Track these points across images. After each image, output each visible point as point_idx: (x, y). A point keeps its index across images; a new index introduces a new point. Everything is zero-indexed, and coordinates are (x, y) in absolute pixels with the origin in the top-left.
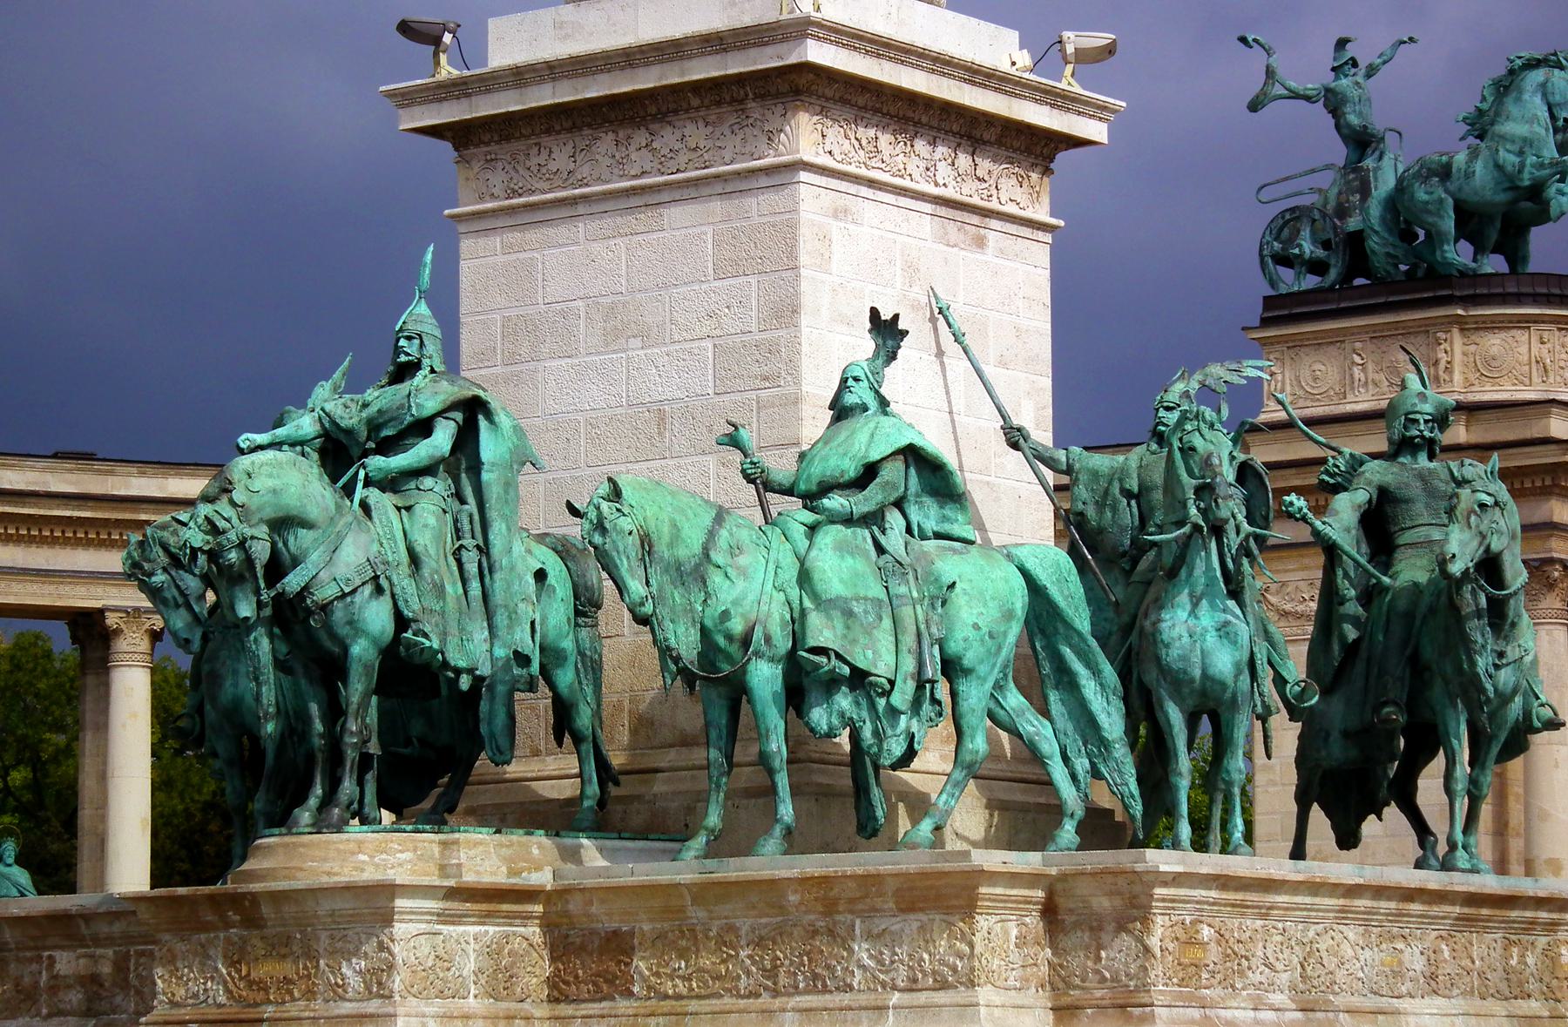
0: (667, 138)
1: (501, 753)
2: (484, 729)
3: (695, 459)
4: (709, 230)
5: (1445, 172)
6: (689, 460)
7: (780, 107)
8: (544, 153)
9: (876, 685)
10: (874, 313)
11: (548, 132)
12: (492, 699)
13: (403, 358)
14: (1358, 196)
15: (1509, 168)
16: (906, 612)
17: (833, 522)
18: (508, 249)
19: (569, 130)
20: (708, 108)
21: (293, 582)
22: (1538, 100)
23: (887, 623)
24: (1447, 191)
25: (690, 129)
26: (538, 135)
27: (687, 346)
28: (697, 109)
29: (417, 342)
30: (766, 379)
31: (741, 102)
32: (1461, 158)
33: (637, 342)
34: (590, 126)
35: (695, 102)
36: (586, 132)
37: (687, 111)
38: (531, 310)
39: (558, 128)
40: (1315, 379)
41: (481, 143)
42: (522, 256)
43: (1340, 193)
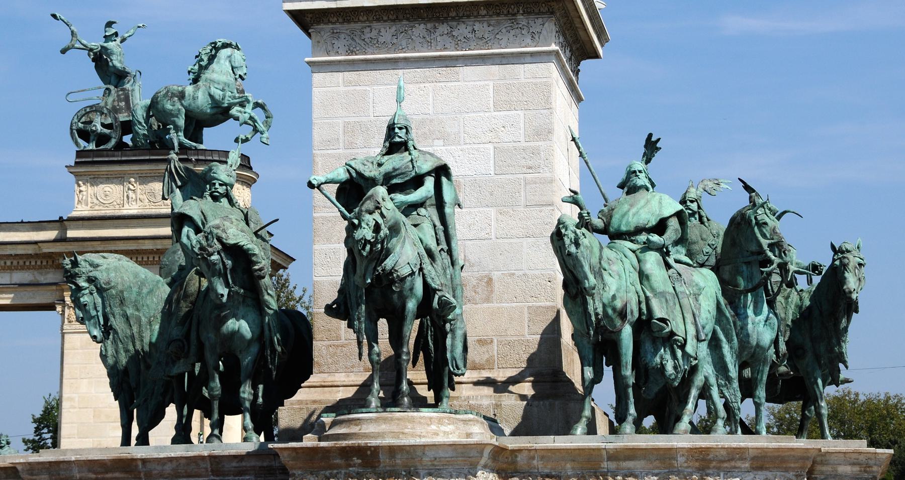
0: (463, 30)
1: (458, 369)
2: (449, 355)
3: (481, 209)
4: (491, 84)
5: (182, 96)
6: (477, 210)
7: (540, 20)
8: (374, 33)
9: (678, 340)
10: (650, 135)
11: (378, 20)
12: (453, 338)
13: (397, 139)
14: (123, 103)
15: (217, 97)
16: (685, 301)
17: (652, 250)
18: (348, 83)
19: (393, 21)
20: (491, 16)
22: (227, 63)
23: (678, 306)
24: (182, 105)
25: (477, 26)
26: (371, 22)
27: (476, 146)
28: (484, 16)
29: (404, 130)
30: (530, 168)
31: (514, 15)
32: (189, 89)
33: (441, 142)
34: (408, 19)
35: (484, 12)
36: (405, 22)
37: (476, 17)
38: (364, 119)
39: (385, 18)
40: (106, 196)
41: (329, 22)
42: (358, 88)
43: (114, 101)
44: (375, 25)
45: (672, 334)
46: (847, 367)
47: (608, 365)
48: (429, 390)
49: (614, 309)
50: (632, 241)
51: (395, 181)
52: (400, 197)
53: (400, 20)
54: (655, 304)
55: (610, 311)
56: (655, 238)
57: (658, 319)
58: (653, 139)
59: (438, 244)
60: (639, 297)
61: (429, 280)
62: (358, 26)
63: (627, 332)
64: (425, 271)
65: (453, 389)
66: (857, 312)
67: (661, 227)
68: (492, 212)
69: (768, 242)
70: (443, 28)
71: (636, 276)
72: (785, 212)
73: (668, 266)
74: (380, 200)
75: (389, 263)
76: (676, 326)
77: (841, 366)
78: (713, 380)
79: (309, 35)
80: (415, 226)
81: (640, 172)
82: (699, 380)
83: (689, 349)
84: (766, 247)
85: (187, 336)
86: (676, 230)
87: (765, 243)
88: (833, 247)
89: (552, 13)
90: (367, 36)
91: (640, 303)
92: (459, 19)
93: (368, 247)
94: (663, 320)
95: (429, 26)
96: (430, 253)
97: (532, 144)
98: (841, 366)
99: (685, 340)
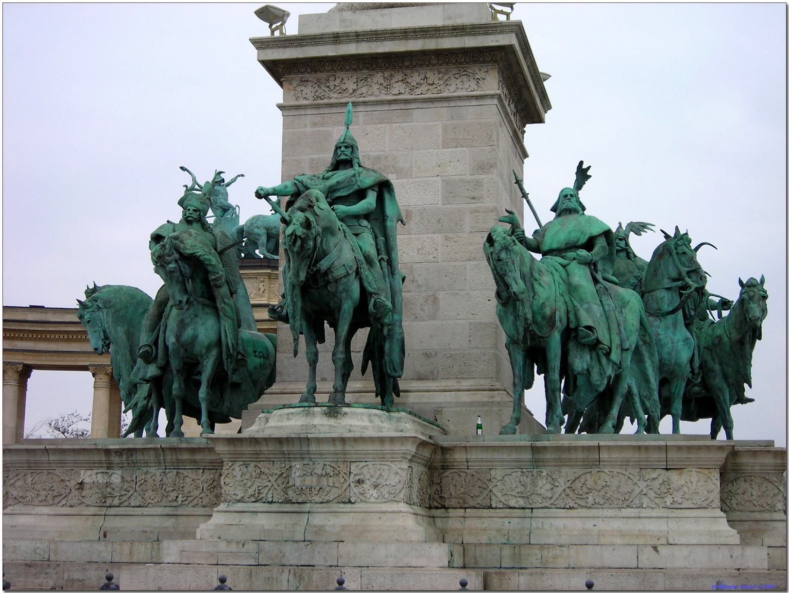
1: (395, 371)
3: (429, 235)
6: (425, 236)
9: (603, 349)
10: (581, 163)
11: (341, 70)
12: (391, 344)
18: (315, 124)
19: (355, 70)
20: (441, 65)
21: (324, 264)
26: (335, 71)
27: (425, 179)
28: (434, 65)
29: (350, 149)
30: (474, 198)
34: (368, 69)
36: (365, 71)
37: (427, 66)
41: (299, 72)
42: (322, 129)
44: (341, 74)
45: (598, 342)
46: (750, 387)
47: (539, 373)
48: (377, 396)
49: (544, 317)
50: (562, 257)
51: (338, 194)
52: (341, 208)
53: (361, 70)
54: (583, 314)
55: (539, 318)
56: (583, 253)
57: (585, 327)
58: (584, 167)
59: (378, 254)
60: (567, 307)
61: (366, 284)
62: (324, 75)
63: (556, 339)
64: (363, 276)
65: (398, 395)
66: (760, 339)
67: (589, 245)
68: (439, 238)
69: (687, 269)
71: (563, 287)
72: (702, 244)
73: (596, 281)
74: (314, 200)
75: (324, 264)
76: (602, 334)
77: (746, 385)
78: (635, 390)
79: (281, 84)
80: (356, 235)
81: (571, 196)
82: (623, 389)
83: (614, 356)
84: (684, 274)
85: (156, 343)
86: (603, 248)
88: (741, 282)
89: (495, 62)
90: (332, 83)
91: (568, 312)
92: (412, 67)
93: (299, 242)
94: (589, 328)
95: (387, 74)
96: (369, 260)
97: (477, 177)
98: (746, 385)
99: (610, 349)
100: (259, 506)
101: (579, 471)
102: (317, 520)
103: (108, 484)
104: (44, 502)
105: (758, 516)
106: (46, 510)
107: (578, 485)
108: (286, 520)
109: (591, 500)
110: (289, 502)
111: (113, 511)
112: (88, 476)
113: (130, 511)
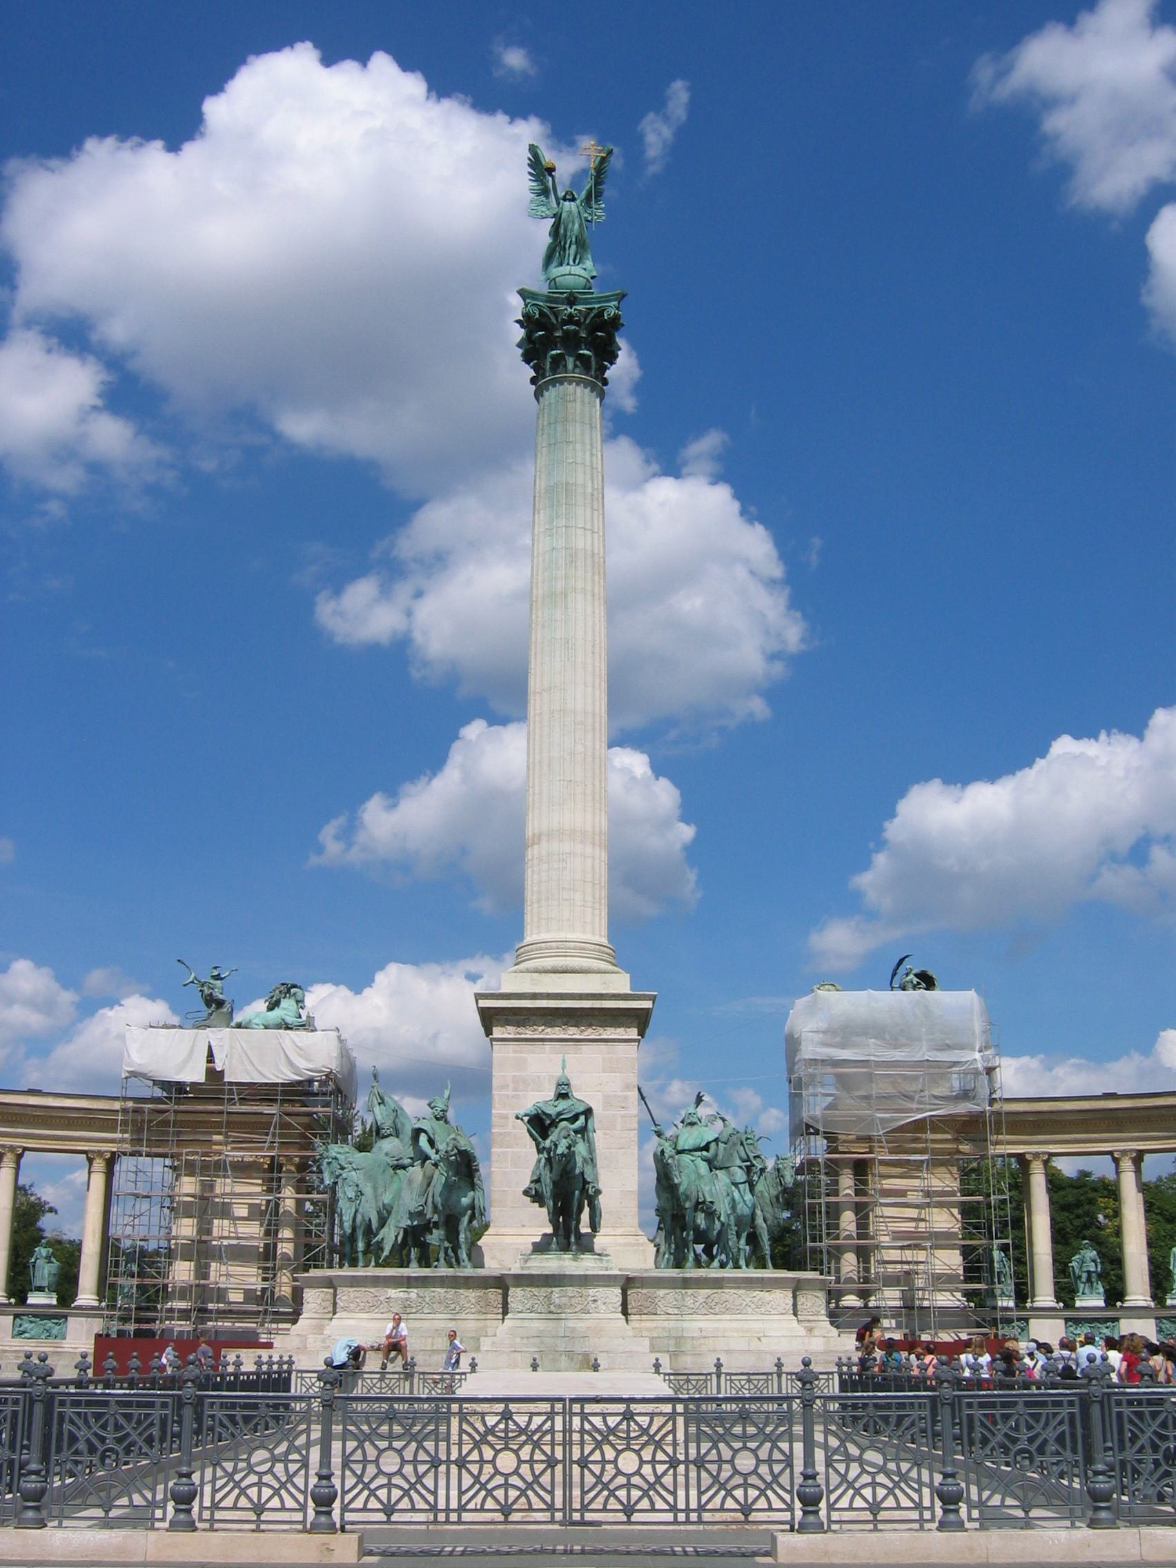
18: (515, 1052)
56: (705, 1153)
67: (706, 1148)
70: (572, 1022)
87: (751, 1155)
100: (533, 1315)
101: (709, 1291)
102: (570, 1324)
103: (407, 1299)
104: (362, 1310)
105: (811, 1318)
106: (365, 1316)
107: (709, 1300)
108: (551, 1324)
109: (717, 1310)
110: (550, 1312)
111: (411, 1316)
112: (393, 1293)
113: (423, 1316)
